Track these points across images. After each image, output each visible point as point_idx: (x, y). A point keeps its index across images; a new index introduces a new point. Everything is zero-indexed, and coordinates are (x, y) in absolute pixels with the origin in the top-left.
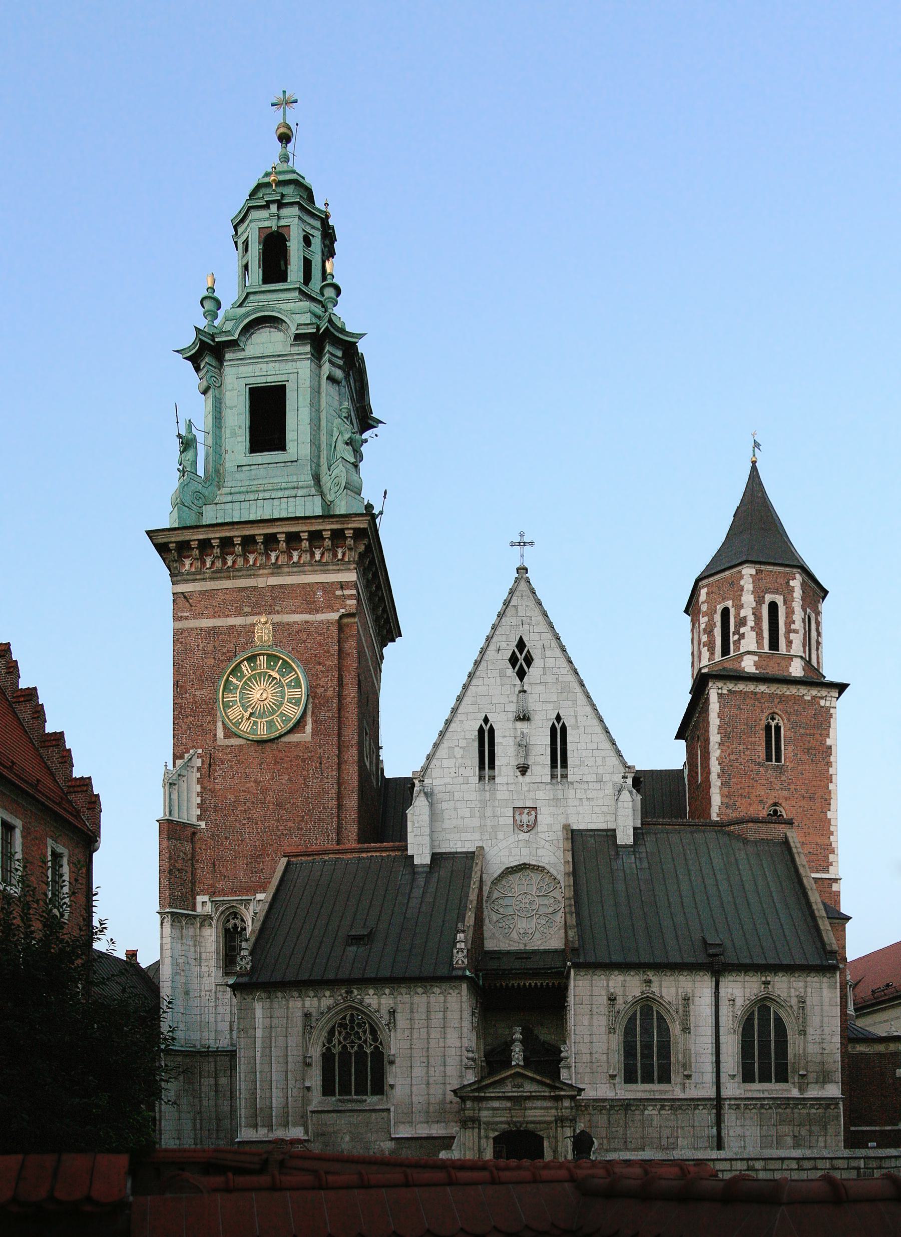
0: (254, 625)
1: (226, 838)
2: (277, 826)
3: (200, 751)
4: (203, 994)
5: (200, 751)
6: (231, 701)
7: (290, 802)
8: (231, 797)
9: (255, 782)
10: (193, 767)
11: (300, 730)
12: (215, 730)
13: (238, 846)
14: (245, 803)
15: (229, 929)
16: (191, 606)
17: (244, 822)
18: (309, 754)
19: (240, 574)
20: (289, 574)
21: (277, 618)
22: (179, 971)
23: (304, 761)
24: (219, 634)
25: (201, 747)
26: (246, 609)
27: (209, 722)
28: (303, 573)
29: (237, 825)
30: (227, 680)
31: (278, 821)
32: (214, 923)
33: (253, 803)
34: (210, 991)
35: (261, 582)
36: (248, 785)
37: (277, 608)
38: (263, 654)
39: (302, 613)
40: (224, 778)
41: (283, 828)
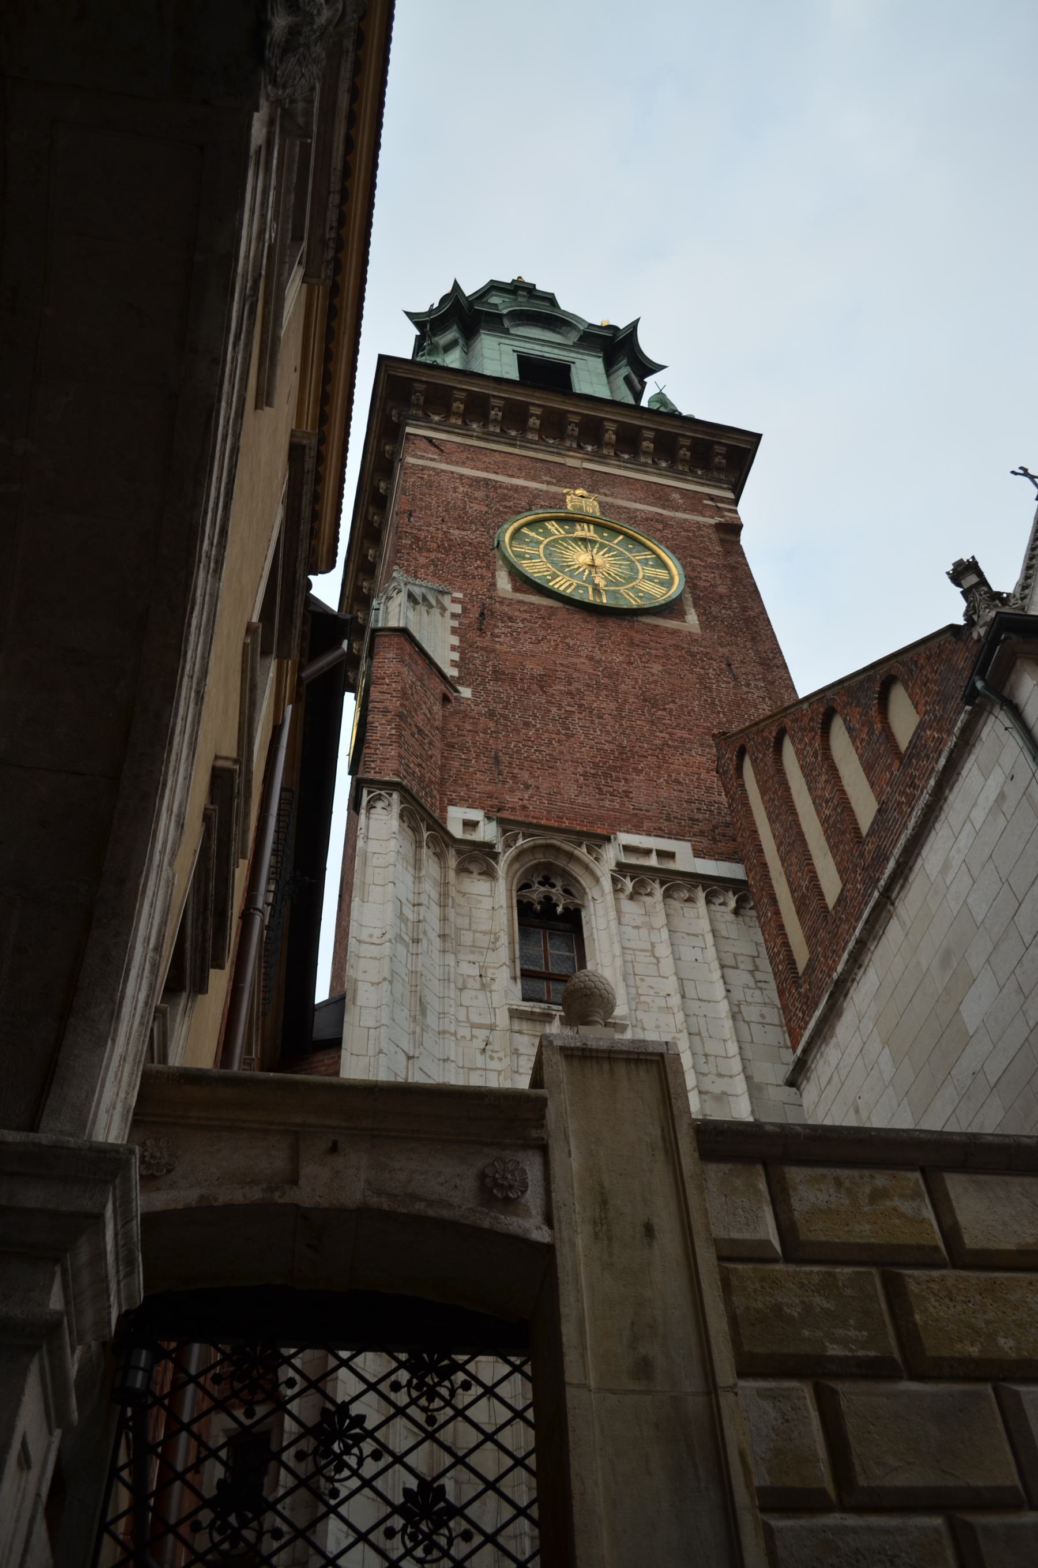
0: (565, 495)
1: (527, 724)
2: (652, 733)
3: (460, 595)
4: (464, 1031)
5: (460, 595)
6: (528, 553)
7: (674, 702)
8: (533, 668)
9: (591, 658)
10: (443, 609)
11: (677, 618)
12: (494, 577)
13: (559, 741)
14: (570, 684)
15: (530, 904)
16: (442, 451)
17: (568, 708)
18: (702, 649)
19: (534, 446)
20: (619, 467)
21: (603, 498)
22: (407, 938)
23: (693, 655)
24: (495, 488)
25: (460, 589)
26: (545, 478)
27: (479, 567)
28: (646, 472)
29: (554, 710)
30: (518, 530)
31: (652, 723)
32: (501, 867)
33: (588, 685)
34: (492, 1028)
35: (570, 462)
36: (570, 659)
37: (602, 491)
38: (589, 522)
39: (647, 504)
40: (517, 640)
41: (667, 736)
